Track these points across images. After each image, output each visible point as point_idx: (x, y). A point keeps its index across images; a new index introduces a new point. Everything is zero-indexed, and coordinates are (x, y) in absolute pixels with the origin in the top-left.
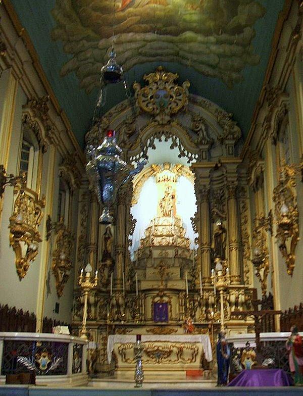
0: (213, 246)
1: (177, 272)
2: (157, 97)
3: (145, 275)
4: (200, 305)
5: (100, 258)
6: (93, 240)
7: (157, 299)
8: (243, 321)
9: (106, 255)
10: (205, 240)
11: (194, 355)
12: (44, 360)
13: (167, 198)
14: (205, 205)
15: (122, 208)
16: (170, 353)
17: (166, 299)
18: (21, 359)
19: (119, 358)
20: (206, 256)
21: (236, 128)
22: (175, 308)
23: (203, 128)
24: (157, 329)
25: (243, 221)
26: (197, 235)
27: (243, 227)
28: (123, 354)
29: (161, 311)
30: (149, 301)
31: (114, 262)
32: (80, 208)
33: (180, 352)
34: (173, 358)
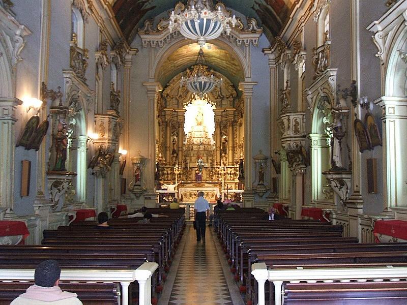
0: (221, 148)
1: (205, 158)
3: (191, 160)
4: (215, 174)
5: (171, 153)
6: (168, 145)
8: (233, 181)
9: (174, 152)
10: (218, 145)
11: (213, 195)
12: (170, 198)
14: (218, 128)
18: (164, 198)
19: (184, 197)
20: (218, 152)
21: (234, 92)
22: (205, 175)
24: (197, 185)
25: (235, 136)
26: (215, 142)
27: (235, 140)
28: (185, 195)
29: (198, 177)
30: (194, 172)
31: (177, 155)
32: (161, 130)
33: (208, 194)
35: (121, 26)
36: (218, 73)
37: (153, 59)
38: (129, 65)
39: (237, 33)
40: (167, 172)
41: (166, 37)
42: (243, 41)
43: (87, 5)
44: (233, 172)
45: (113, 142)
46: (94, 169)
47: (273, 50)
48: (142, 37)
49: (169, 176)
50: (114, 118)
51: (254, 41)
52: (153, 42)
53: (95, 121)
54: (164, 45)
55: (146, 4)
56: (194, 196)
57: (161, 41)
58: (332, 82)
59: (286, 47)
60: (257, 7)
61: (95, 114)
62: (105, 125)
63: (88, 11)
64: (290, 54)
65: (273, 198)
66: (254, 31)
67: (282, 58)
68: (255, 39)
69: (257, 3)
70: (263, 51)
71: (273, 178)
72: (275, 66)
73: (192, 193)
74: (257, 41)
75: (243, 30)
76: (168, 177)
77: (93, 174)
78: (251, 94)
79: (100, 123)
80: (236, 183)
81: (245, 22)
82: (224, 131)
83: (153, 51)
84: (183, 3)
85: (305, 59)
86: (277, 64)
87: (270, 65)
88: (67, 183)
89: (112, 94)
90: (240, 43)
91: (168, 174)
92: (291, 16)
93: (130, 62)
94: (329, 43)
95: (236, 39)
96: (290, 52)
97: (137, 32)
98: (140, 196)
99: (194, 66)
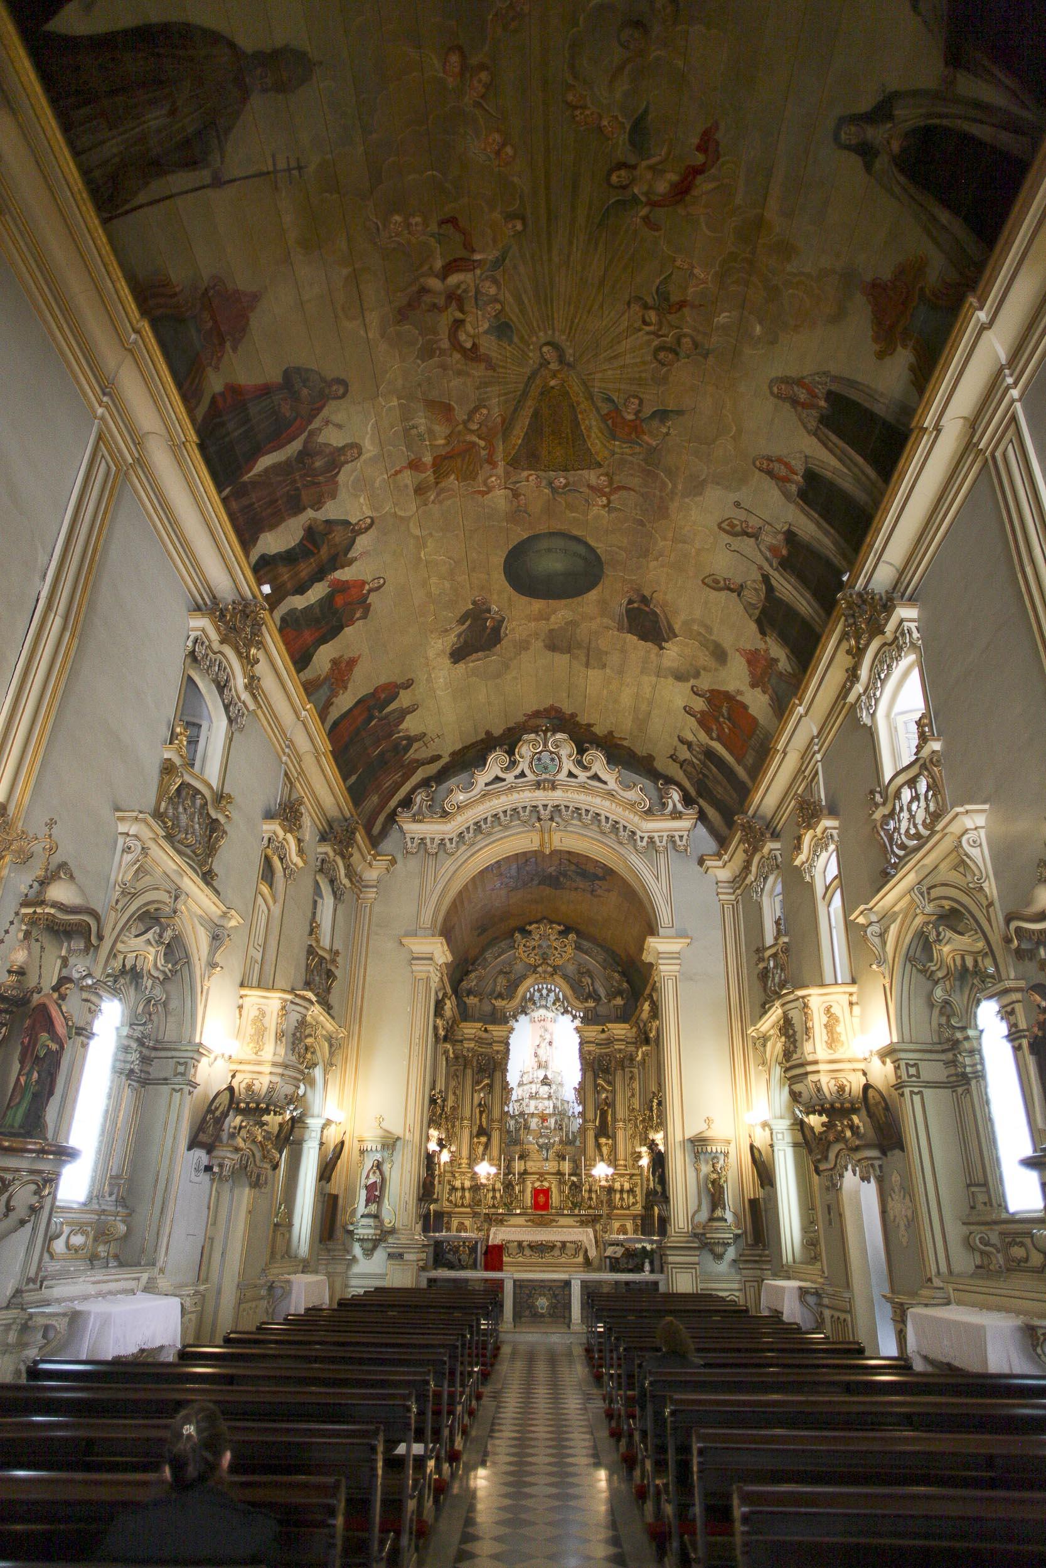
2: (540, 946)
7: (537, 1184)
10: (590, 1115)
13: (543, 1045)
14: (590, 1074)
15: (498, 1074)
16: (553, 1247)
17: (546, 1184)
20: (591, 1134)
21: (625, 985)
23: (590, 981)
26: (580, 1109)
31: (489, 1140)
34: (556, 1252)
35: (350, 789)
36: (586, 944)
37: (431, 878)
38: (371, 894)
39: (636, 819)
40: (462, 1184)
41: (463, 828)
42: (651, 838)
43: (240, 681)
44: (627, 1186)
45: (287, 1072)
46: (215, 1153)
47: (726, 857)
48: (406, 827)
49: (467, 1194)
50: (297, 1000)
51: (677, 838)
52: (433, 839)
53: (241, 1007)
54: (458, 848)
55: (416, 745)
56: (527, 1252)
57: (451, 840)
58: (974, 852)
59: (768, 835)
60: (684, 754)
61: (242, 985)
62: (266, 1021)
63: (245, 696)
64: (778, 853)
65: (756, 1262)
66: (676, 815)
67: (754, 869)
68: (681, 833)
69: (682, 741)
70: (701, 862)
71: (750, 1201)
72: (733, 897)
73: (525, 1244)
74: (685, 837)
75: (649, 812)
76: (463, 1197)
77: (208, 1169)
78: (677, 968)
79: (254, 1013)
80: (635, 1217)
81: (654, 794)
82: (604, 1080)
83: (431, 862)
84: (506, 752)
85: (836, 838)
86: (739, 892)
87: (722, 897)
88: (33, 1187)
89: (311, 951)
90: (644, 843)
91: (463, 1189)
92: (780, 747)
93: (376, 887)
94: (936, 746)
95: (634, 833)
96: (777, 845)
97: (392, 818)
98: (375, 1248)
99: (531, 924)
